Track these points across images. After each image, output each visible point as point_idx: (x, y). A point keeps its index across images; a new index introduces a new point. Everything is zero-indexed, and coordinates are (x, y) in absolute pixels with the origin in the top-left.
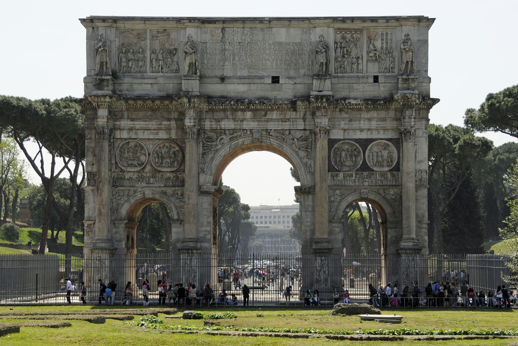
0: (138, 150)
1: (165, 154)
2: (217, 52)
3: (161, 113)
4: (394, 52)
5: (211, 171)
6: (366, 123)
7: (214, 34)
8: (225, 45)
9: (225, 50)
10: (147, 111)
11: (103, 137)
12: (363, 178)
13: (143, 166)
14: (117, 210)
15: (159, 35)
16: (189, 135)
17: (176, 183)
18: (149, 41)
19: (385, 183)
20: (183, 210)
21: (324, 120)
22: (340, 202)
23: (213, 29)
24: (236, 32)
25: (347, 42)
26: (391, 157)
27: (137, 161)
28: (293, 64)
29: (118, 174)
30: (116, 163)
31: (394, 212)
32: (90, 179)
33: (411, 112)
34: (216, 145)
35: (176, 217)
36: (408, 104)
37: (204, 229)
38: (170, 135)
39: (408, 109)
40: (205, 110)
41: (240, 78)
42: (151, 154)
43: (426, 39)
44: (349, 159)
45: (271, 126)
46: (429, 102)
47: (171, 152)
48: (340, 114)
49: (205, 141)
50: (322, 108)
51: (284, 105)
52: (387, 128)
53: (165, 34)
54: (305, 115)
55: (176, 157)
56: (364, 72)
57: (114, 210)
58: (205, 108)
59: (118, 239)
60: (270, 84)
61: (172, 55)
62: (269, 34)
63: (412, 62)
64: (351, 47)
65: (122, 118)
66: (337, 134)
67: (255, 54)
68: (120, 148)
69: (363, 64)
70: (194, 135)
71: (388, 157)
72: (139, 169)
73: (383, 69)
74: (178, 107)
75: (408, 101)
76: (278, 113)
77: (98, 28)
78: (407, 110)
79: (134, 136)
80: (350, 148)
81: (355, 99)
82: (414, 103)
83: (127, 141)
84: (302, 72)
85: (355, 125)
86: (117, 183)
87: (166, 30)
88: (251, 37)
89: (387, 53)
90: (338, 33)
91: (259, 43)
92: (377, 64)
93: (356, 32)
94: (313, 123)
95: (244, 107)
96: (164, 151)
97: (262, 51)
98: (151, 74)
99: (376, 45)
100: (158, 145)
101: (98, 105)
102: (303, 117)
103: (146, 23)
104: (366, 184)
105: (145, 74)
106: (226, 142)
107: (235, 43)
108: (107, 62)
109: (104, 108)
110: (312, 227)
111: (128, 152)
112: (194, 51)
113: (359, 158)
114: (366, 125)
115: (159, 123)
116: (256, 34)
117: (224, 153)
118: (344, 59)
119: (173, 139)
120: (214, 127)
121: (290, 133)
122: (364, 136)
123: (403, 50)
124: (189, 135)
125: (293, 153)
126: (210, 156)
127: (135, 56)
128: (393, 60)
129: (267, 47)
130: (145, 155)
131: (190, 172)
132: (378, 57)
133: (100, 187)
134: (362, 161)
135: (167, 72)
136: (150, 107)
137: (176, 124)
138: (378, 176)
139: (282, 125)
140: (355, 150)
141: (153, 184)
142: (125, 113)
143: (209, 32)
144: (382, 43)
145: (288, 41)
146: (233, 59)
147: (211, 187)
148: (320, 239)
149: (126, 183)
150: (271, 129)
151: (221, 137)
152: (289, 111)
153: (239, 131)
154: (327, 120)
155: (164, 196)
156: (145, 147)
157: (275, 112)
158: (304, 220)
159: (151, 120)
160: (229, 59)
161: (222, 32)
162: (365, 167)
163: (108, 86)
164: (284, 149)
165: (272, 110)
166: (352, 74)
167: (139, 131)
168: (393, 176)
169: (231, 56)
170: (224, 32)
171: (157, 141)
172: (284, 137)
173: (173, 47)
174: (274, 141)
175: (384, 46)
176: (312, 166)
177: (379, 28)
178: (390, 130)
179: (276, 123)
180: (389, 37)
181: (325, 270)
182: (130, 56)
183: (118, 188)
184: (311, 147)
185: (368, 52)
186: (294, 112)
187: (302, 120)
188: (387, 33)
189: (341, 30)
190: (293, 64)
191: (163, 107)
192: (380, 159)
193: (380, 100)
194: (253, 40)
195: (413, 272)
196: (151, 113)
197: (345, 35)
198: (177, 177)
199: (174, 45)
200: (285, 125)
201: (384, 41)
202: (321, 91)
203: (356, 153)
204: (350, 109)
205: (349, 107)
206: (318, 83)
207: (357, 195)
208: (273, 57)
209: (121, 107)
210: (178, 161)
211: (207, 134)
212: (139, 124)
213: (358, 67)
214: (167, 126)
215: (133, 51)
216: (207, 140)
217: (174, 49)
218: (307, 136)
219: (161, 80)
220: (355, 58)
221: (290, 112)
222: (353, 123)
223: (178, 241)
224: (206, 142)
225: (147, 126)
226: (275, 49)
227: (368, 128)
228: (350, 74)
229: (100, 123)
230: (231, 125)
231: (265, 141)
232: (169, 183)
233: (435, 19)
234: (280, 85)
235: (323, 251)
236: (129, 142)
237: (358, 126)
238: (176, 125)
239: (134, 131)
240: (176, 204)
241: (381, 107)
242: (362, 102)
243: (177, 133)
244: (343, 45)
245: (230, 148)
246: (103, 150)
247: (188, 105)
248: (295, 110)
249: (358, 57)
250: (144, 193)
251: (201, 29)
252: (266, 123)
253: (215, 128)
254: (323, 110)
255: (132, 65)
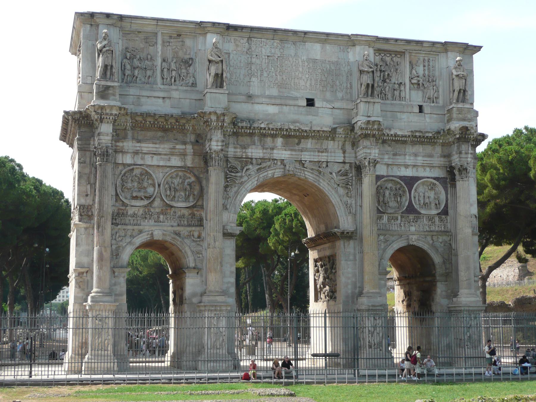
0: (144, 179)
1: (178, 185)
2: (242, 65)
3: (174, 135)
4: (437, 81)
5: (235, 208)
6: (412, 158)
7: (239, 44)
8: (251, 58)
9: (251, 63)
10: (156, 131)
11: (107, 159)
12: (409, 222)
13: (152, 199)
14: (117, 255)
15: (172, 40)
16: (215, 161)
17: (192, 221)
18: (160, 47)
19: (433, 228)
20: (201, 256)
21: (373, 150)
22: (384, 250)
23: (237, 38)
24: (265, 44)
25: (387, 65)
26: (438, 199)
27: (144, 192)
28: (329, 85)
29: (119, 209)
30: (117, 195)
31: (444, 263)
32: (83, 214)
33: (467, 146)
34: (241, 177)
35: (192, 265)
36: (465, 137)
37: (226, 280)
38: (184, 162)
39: (464, 143)
40: (228, 134)
41: (270, 97)
42: (161, 185)
43: (470, 69)
44: (393, 199)
45: (306, 157)
46: (479, 138)
47: (186, 183)
48: (383, 146)
49: (228, 172)
50: (371, 136)
51: (321, 133)
52: (434, 165)
53: (178, 40)
54: (344, 145)
55: (192, 190)
56: (407, 100)
57: (116, 254)
58: (229, 130)
59: (117, 293)
60: (304, 106)
61: (187, 65)
62: (303, 48)
63: (465, 91)
64: (392, 70)
65: (125, 138)
66: (381, 170)
67: (286, 71)
68: (122, 176)
69: (407, 90)
70: (221, 161)
71: (435, 199)
72: (146, 202)
73: (426, 99)
74: (196, 128)
75: (466, 134)
76: (314, 141)
77: (98, 26)
78: (463, 144)
79: (140, 162)
80: (394, 187)
81: (401, 130)
82: (472, 137)
83: (131, 167)
84: (340, 95)
85: (400, 160)
86: (117, 220)
87: (180, 35)
88: (282, 51)
89: (430, 81)
90: (377, 54)
91: (291, 59)
92: (420, 93)
93: (396, 55)
94: (354, 155)
95: (275, 132)
96: (176, 181)
97: (294, 68)
98: (162, 87)
99: (417, 70)
100: (170, 174)
101: (101, 118)
102: (342, 147)
103: (159, 24)
104: (413, 229)
105: (154, 86)
106: (253, 173)
107: (263, 57)
108: (112, 66)
109: (108, 122)
110: (354, 280)
111: (132, 181)
112: (221, 59)
113: (404, 199)
114: (412, 161)
115: (171, 146)
116: (287, 47)
117: (250, 187)
118: (385, 84)
119: (189, 167)
120: (239, 154)
121: (327, 166)
122: (409, 173)
123: (454, 77)
124: (215, 161)
125: (331, 190)
126: (235, 189)
127: (142, 63)
128: (436, 89)
129: (300, 63)
130: (154, 186)
131: (216, 207)
132: (421, 84)
133: (101, 223)
134: (408, 201)
135: (181, 86)
136: (161, 126)
137: (193, 149)
138: (425, 220)
139: (319, 156)
140: (399, 189)
141: (163, 222)
142: (128, 132)
143: (233, 41)
144: (424, 70)
145: (323, 59)
146: (261, 75)
147: (235, 228)
148: (372, 293)
149: (130, 220)
150: (306, 159)
151: (247, 167)
152: (326, 139)
153: (268, 160)
154: (377, 151)
155: (178, 238)
156: (154, 176)
157: (310, 140)
158: (345, 271)
159: (161, 142)
160: (256, 74)
161: (248, 41)
162: (411, 209)
163: (114, 95)
164: (321, 185)
165: (307, 137)
166: (395, 102)
167: (146, 156)
168: (441, 220)
169: (259, 71)
170: (250, 43)
171: (168, 169)
172: (320, 169)
173: (188, 57)
174: (310, 174)
175: (426, 72)
176: (354, 205)
177: (422, 52)
178: (437, 168)
179: (312, 153)
180: (431, 64)
181: (378, 331)
182: (136, 63)
183: (119, 227)
184: (352, 183)
185: (411, 79)
186: (332, 142)
187: (341, 151)
188: (429, 59)
189: (380, 52)
190: (329, 85)
191: (178, 127)
192: (427, 201)
193: (429, 132)
194: (283, 55)
195: (476, 333)
196: (162, 134)
197: (384, 57)
198: (193, 215)
199: (189, 54)
200: (322, 156)
201: (426, 68)
202: (369, 117)
203: (401, 192)
204: (395, 141)
205: (394, 139)
206: (366, 108)
207: (403, 242)
208: (307, 76)
209: (125, 125)
210: (194, 195)
211: (230, 162)
212: (146, 147)
213: (400, 94)
214: (181, 151)
215: (140, 58)
216: (230, 169)
217: (190, 59)
218: (347, 170)
219: (175, 94)
220: (398, 84)
221: (327, 141)
222: (398, 157)
223: (194, 295)
224: (229, 172)
225: (157, 150)
226: (309, 67)
227: (413, 164)
228: (393, 102)
229: (104, 141)
230: (259, 153)
231: (299, 174)
232: (184, 221)
233: (481, 47)
234: (316, 109)
235: (378, 308)
236: (133, 169)
237: (403, 161)
238: (192, 151)
239: (140, 155)
240: (192, 249)
241: (428, 141)
242: (410, 134)
243: (193, 160)
244: (383, 69)
245: (257, 180)
246: (106, 176)
247: (215, 124)
248: (333, 139)
249: (401, 83)
250: (152, 234)
251: (223, 37)
252: (300, 153)
253: (240, 156)
254: (372, 139)
255: (138, 74)
